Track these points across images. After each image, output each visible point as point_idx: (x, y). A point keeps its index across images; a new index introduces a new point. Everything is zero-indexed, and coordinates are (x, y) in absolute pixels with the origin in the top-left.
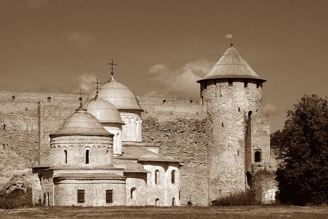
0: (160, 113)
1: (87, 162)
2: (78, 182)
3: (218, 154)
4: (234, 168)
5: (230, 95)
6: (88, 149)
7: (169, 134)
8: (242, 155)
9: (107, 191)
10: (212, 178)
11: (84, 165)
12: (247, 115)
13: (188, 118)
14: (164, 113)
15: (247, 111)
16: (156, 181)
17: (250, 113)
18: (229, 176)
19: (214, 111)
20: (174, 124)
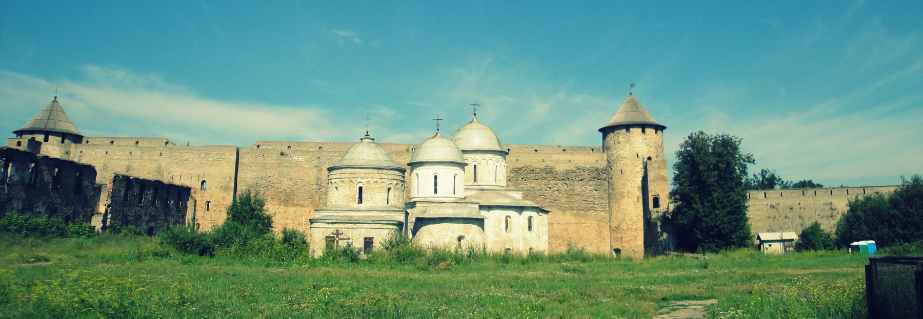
0: (558, 162)
1: (360, 201)
2: (326, 225)
3: (617, 201)
4: (634, 215)
5: (628, 141)
6: (360, 185)
7: (567, 182)
8: (641, 200)
9: (366, 239)
10: (614, 225)
11: (355, 205)
12: (646, 160)
13: (588, 166)
14: (562, 162)
15: (646, 157)
16: (507, 227)
17: (649, 158)
18: (629, 223)
19: (613, 158)
20: (574, 172)
